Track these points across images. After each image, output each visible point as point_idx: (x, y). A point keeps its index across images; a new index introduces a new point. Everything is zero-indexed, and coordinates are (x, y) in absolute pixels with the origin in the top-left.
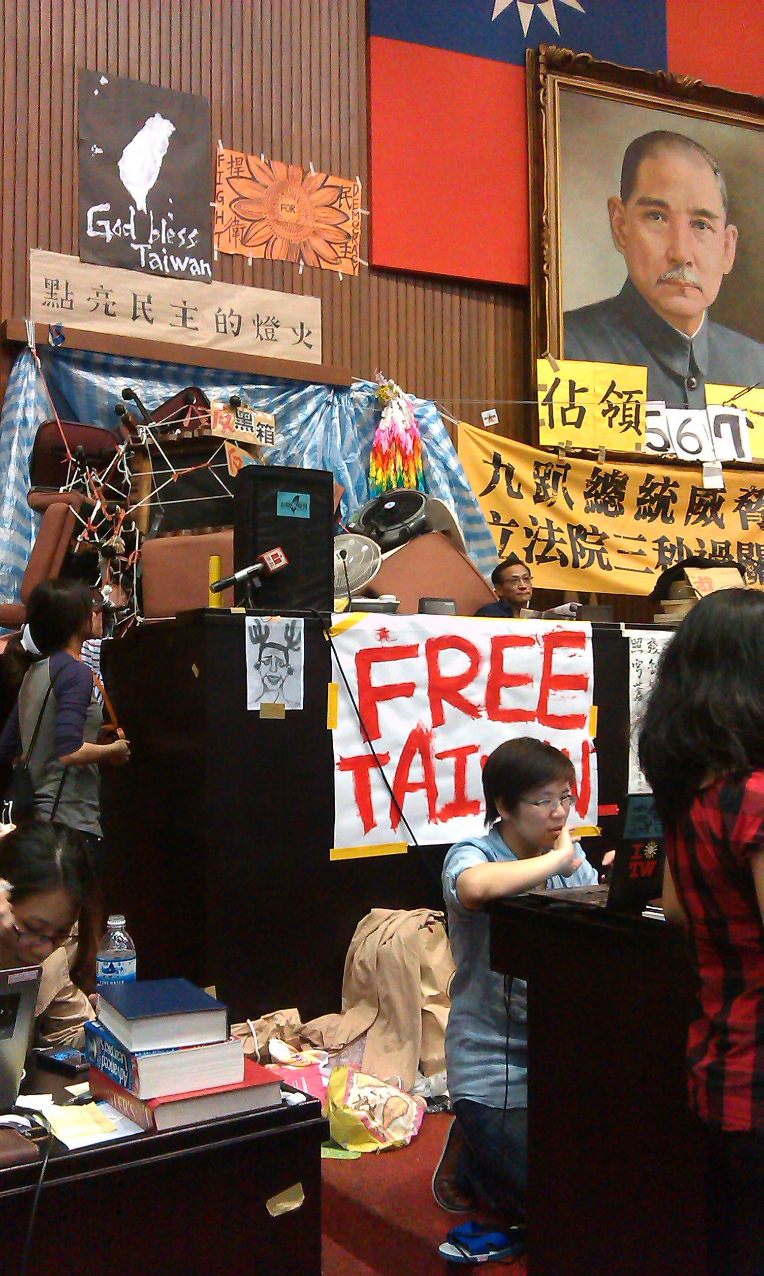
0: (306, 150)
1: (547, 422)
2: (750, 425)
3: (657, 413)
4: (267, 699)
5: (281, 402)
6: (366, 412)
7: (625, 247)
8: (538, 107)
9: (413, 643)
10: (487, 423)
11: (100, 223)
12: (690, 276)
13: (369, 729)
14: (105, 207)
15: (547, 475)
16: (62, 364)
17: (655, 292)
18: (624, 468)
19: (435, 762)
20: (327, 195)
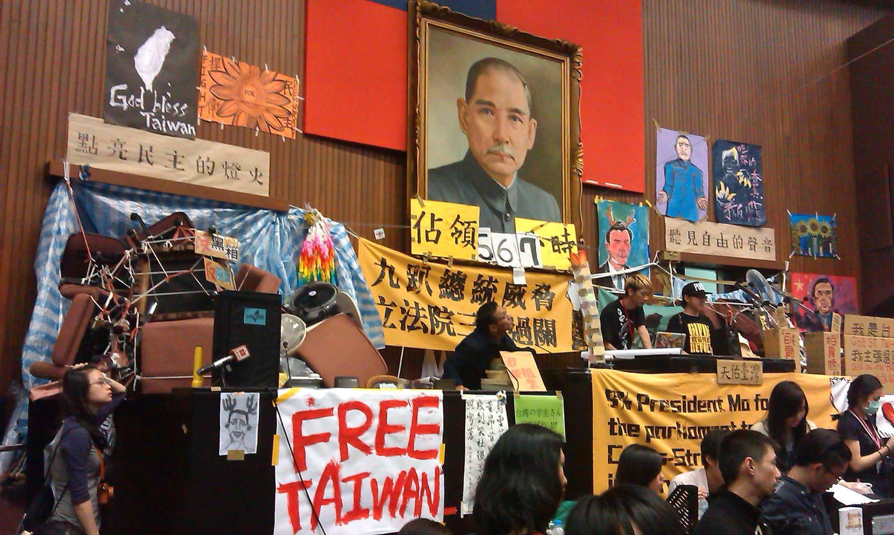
0: (263, 55)
1: (416, 239)
2: (542, 244)
3: (486, 235)
4: (233, 447)
5: (240, 220)
6: (298, 229)
7: (467, 130)
8: (415, 40)
9: (330, 407)
10: (377, 237)
11: (119, 97)
12: (507, 150)
13: (299, 464)
14: (124, 87)
15: (416, 273)
16: (88, 192)
17: (485, 160)
18: (465, 270)
19: (342, 484)
20: (276, 86)
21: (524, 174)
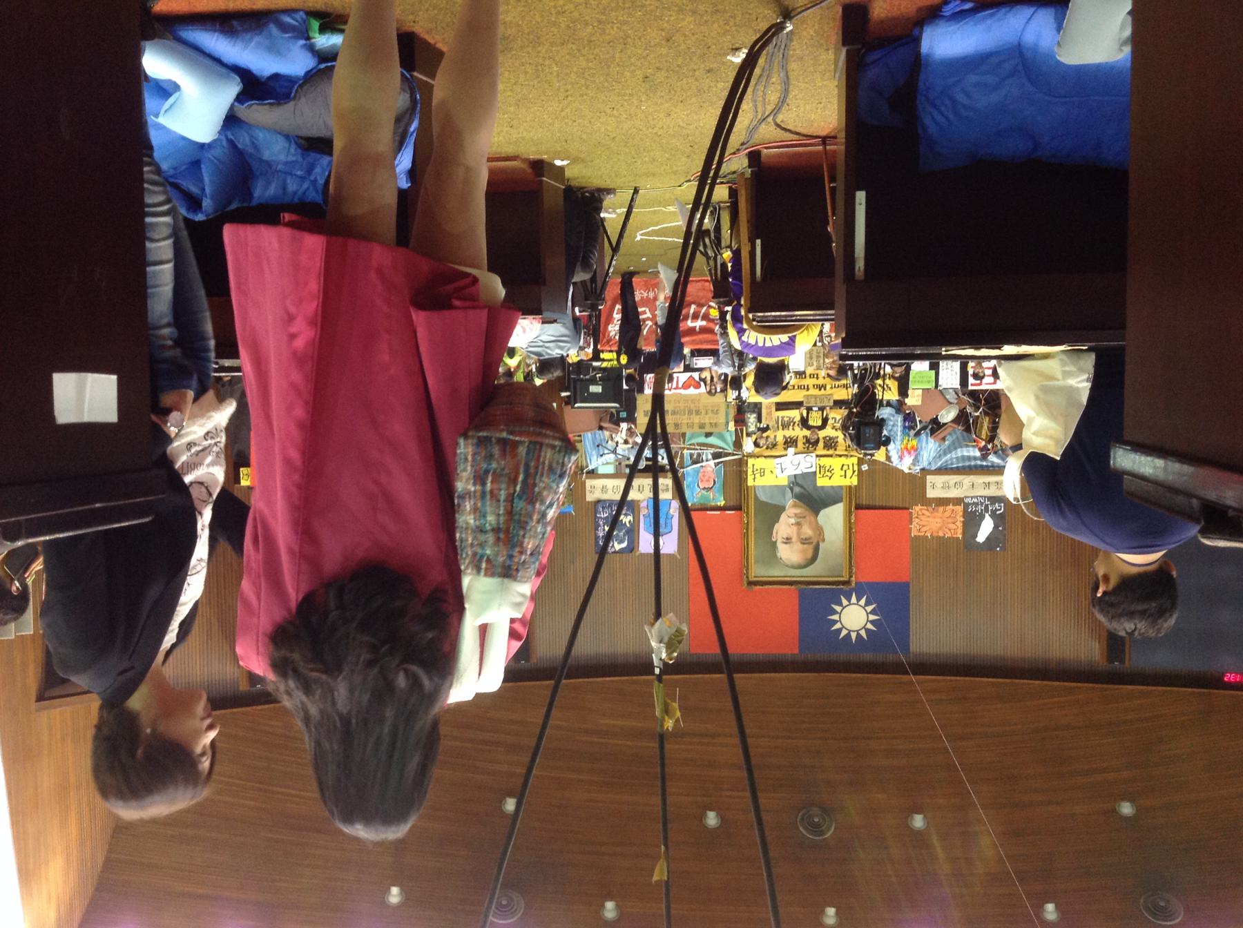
12: (793, 521)
20: (924, 529)
21: (781, 509)
